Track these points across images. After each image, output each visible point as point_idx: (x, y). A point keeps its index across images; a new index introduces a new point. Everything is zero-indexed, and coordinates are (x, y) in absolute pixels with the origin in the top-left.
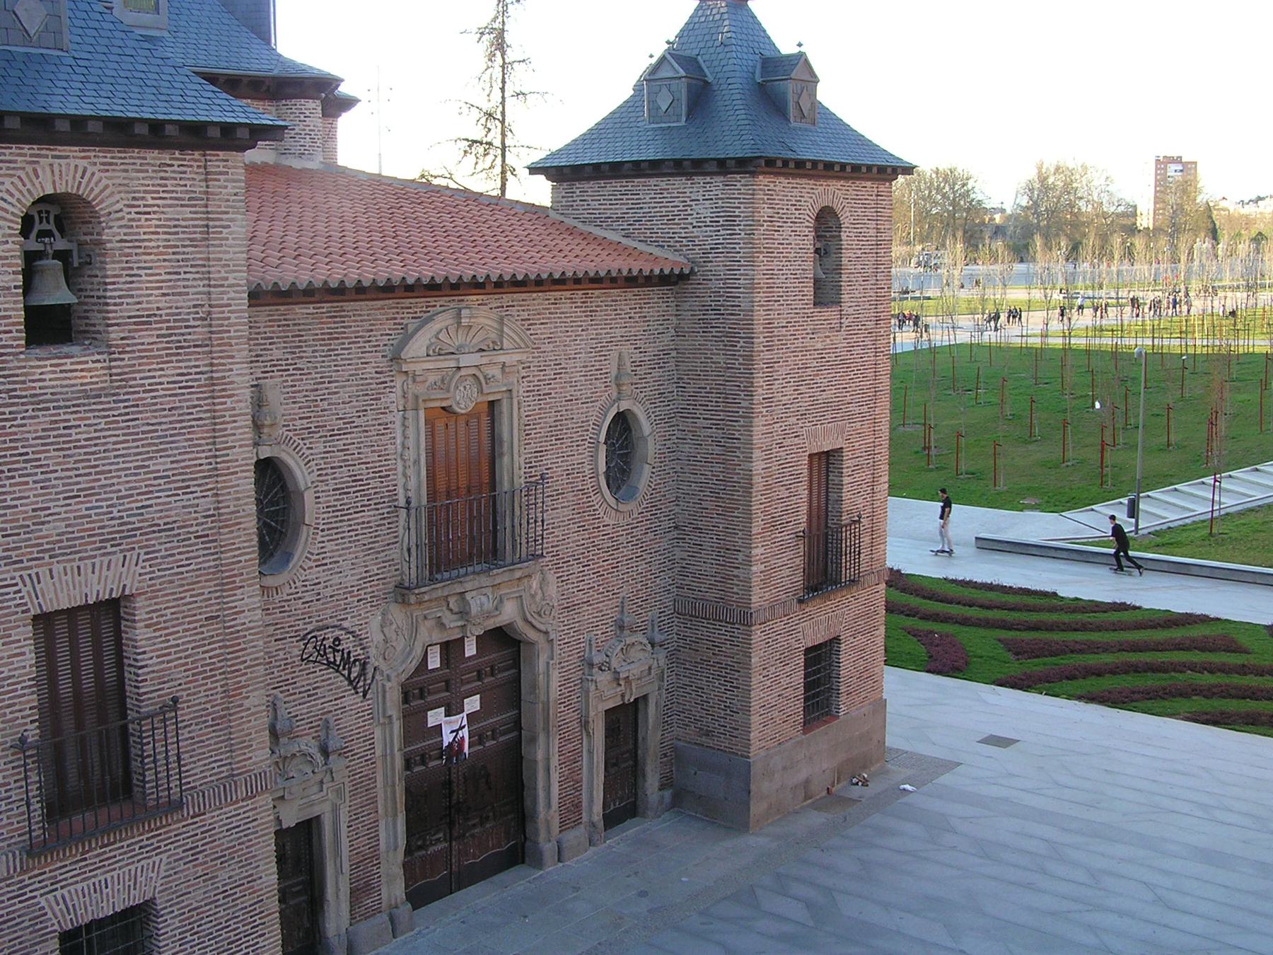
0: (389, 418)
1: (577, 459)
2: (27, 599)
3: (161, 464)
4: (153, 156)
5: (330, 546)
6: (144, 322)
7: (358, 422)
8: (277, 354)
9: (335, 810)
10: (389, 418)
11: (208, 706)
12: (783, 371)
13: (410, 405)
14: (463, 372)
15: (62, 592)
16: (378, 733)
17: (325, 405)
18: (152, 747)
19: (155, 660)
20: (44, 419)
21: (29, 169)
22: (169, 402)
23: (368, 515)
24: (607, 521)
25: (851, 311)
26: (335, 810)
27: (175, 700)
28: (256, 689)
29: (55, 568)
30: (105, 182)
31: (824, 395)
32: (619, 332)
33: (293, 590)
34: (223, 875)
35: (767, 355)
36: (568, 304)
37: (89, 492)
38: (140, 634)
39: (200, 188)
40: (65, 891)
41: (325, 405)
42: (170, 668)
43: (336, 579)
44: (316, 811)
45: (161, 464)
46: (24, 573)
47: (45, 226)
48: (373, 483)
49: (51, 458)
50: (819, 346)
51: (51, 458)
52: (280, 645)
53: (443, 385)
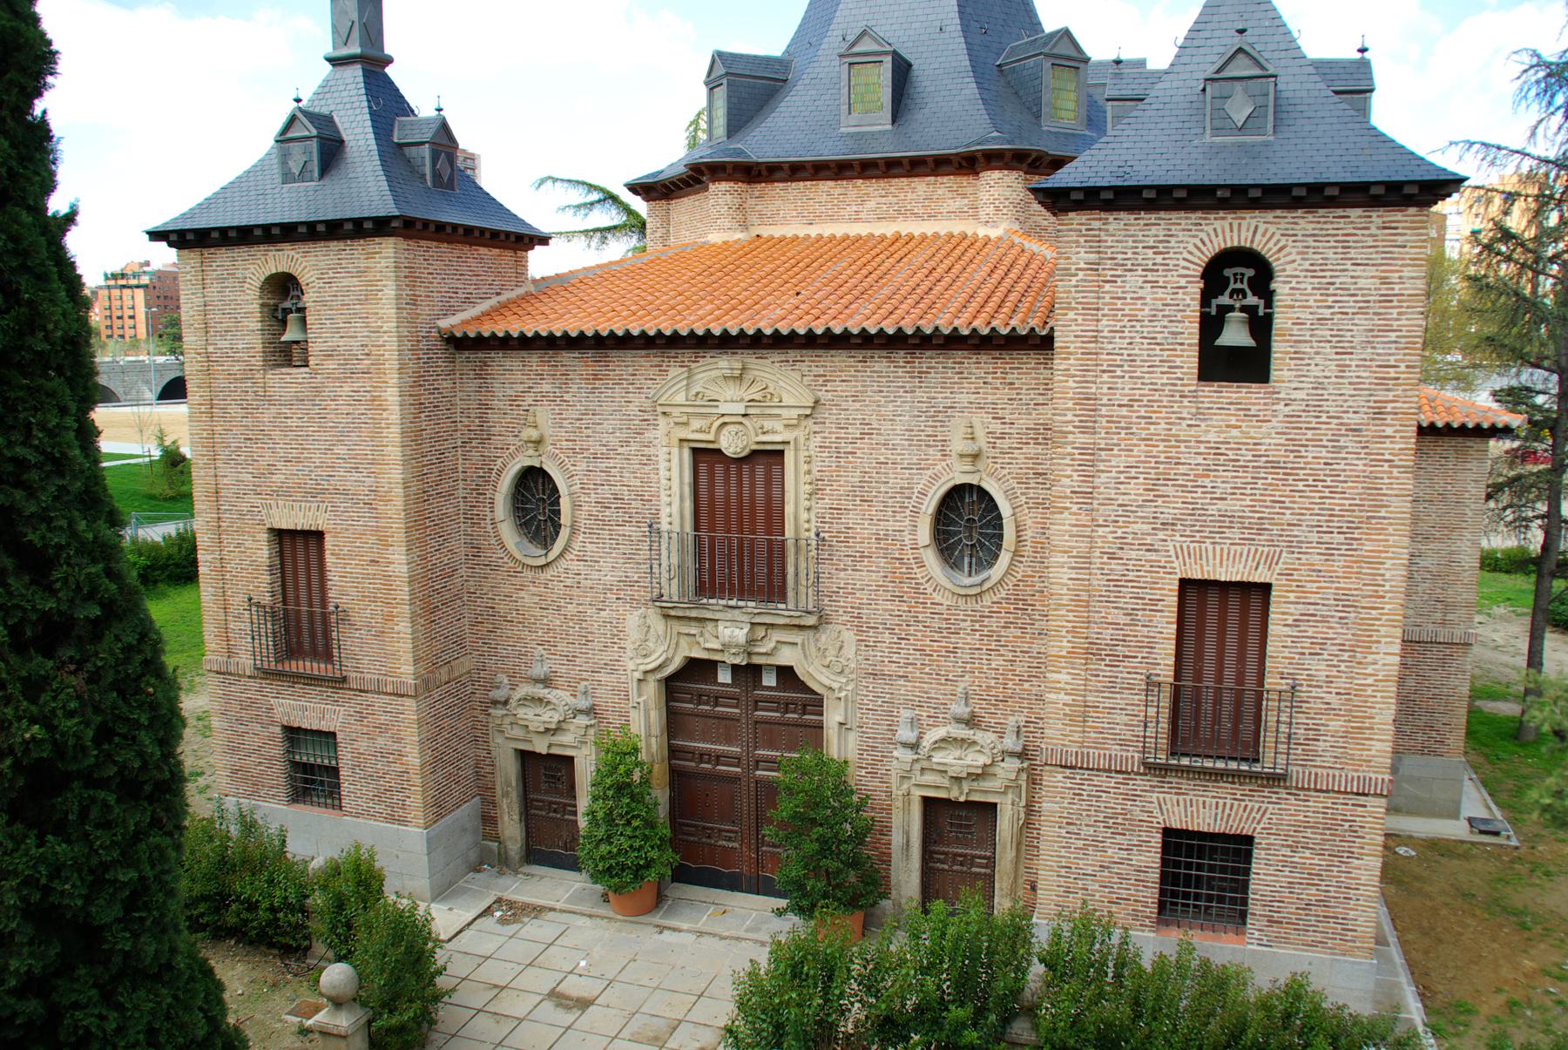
0: (652, 451)
1: (891, 526)
3: (341, 450)
4: (334, 245)
7: (620, 450)
8: (546, 387)
10: (652, 451)
12: (1119, 461)
20: (273, 410)
22: (345, 409)
24: (938, 599)
25: (1301, 395)
31: (1221, 505)
32: (964, 398)
34: (380, 741)
35: (1082, 439)
36: (979, 367)
43: (595, 575)
45: (341, 450)
50: (1212, 437)
51: (276, 435)
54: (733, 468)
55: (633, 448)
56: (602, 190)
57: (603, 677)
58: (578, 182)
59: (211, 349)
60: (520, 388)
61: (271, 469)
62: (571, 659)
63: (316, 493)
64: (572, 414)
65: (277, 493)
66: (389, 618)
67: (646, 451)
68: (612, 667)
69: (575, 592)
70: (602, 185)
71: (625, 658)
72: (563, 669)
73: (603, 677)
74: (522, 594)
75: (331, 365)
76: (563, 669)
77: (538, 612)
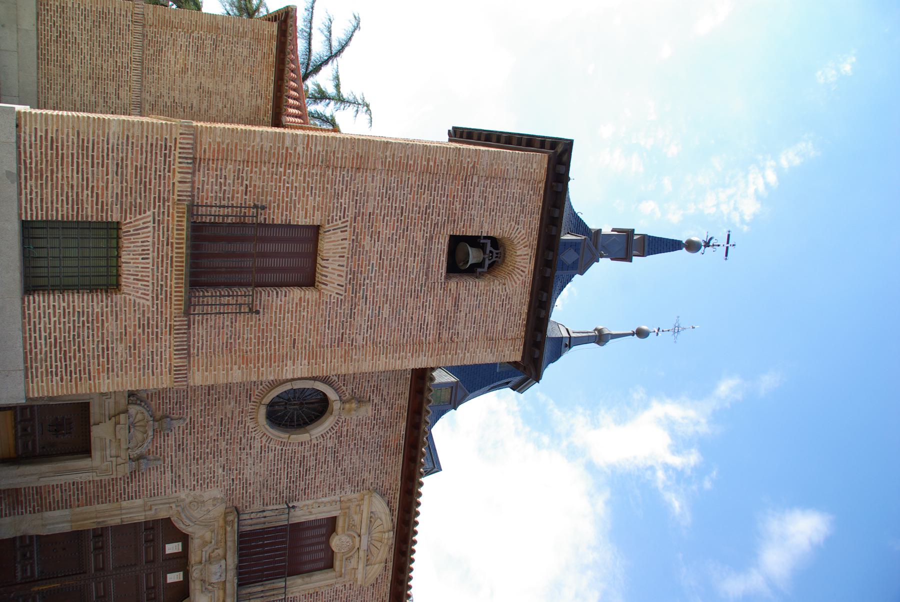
2: (335, 223)
3: (386, 312)
5: (271, 455)
6: (456, 304)
7: (339, 469)
8: (383, 412)
9: (92, 470)
10: (338, 491)
11: (241, 340)
13: (344, 505)
14: (357, 539)
15: (332, 246)
16: (138, 502)
17: (352, 446)
18: (227, 297)
19: (279, 303)
20: (421, 242)
21: (528, 243)
22: (415, 317)
23: (284, 481)
26: (92, 470)
27: (258, 312)
28: (243, 375)
29: (347, 242)
30: (518, 282)
33: (250, 430)
34: (120, 348)
37: (381, 266)
38: (296, 293)
39: (509, 335)
40: (151, 229)
41: (352, 446)
42: (271, 313)
43: (250, 461)
44: (96, 453)
45: (386, 312)
46: (348, 224)
47: (495, 255)
48: (302, 483)
49: (402, 245)
51: (402, 245)
52: (218, 422)
53: (351, 527)
54: (323, 539)
55: (341, 478)
56: (340, 51)
57: (169, 475)
58: (350, 39)
59: (475, 180)
60: (385, 393)
61: (376, 235)
62: (180, 447)
63: (354, 281)
64: (366, 433)
65: (356, 242)
66: (246, 361)
67: (338, 487)
68: (177, 481)
69: (237, 447)
70: (343, 54)
71: (187, 491)
72: (171, 442)
73: (169, 475)
74: (233, 403)
75: (449, 304)
76: (171, 442)
77: (218, 417)
